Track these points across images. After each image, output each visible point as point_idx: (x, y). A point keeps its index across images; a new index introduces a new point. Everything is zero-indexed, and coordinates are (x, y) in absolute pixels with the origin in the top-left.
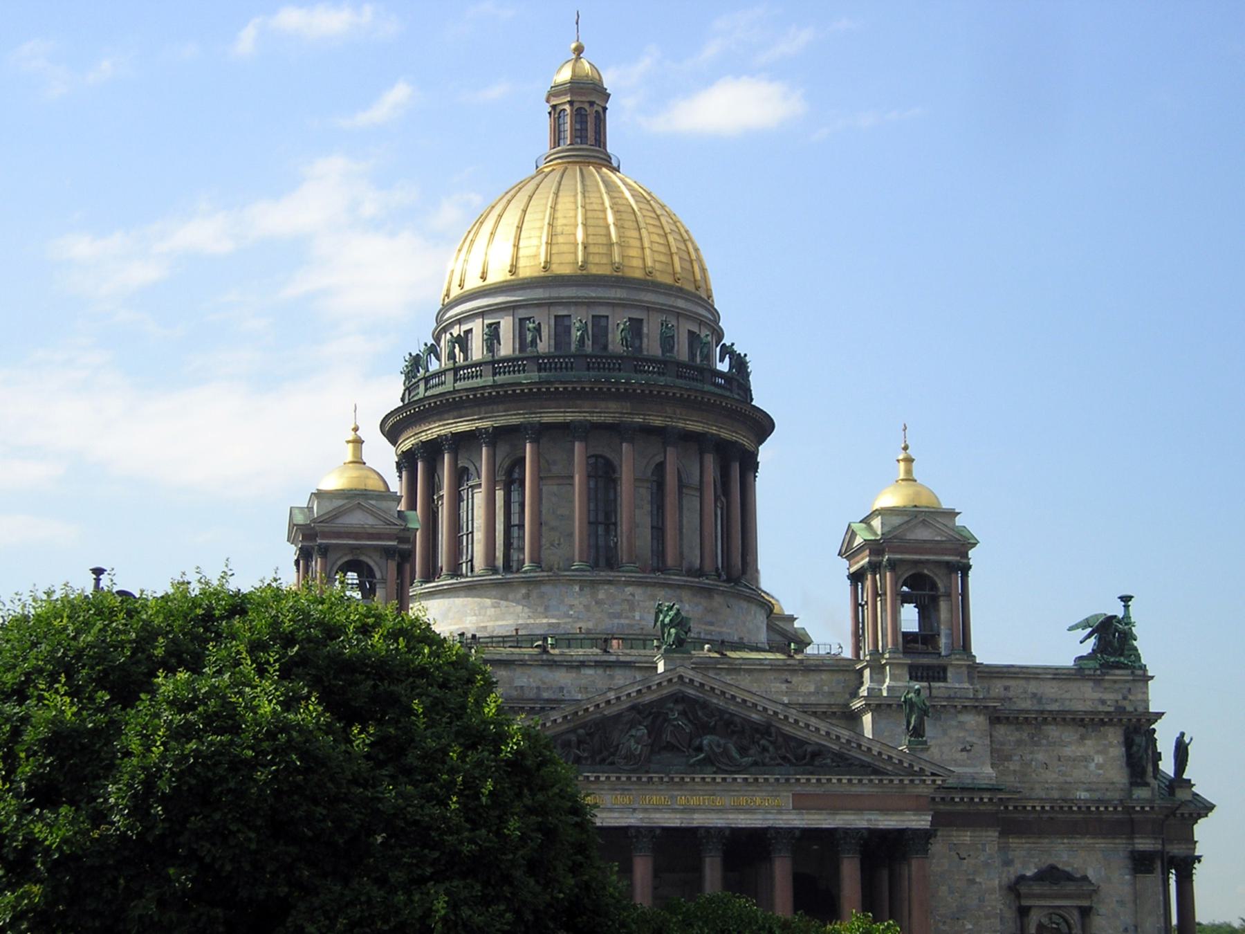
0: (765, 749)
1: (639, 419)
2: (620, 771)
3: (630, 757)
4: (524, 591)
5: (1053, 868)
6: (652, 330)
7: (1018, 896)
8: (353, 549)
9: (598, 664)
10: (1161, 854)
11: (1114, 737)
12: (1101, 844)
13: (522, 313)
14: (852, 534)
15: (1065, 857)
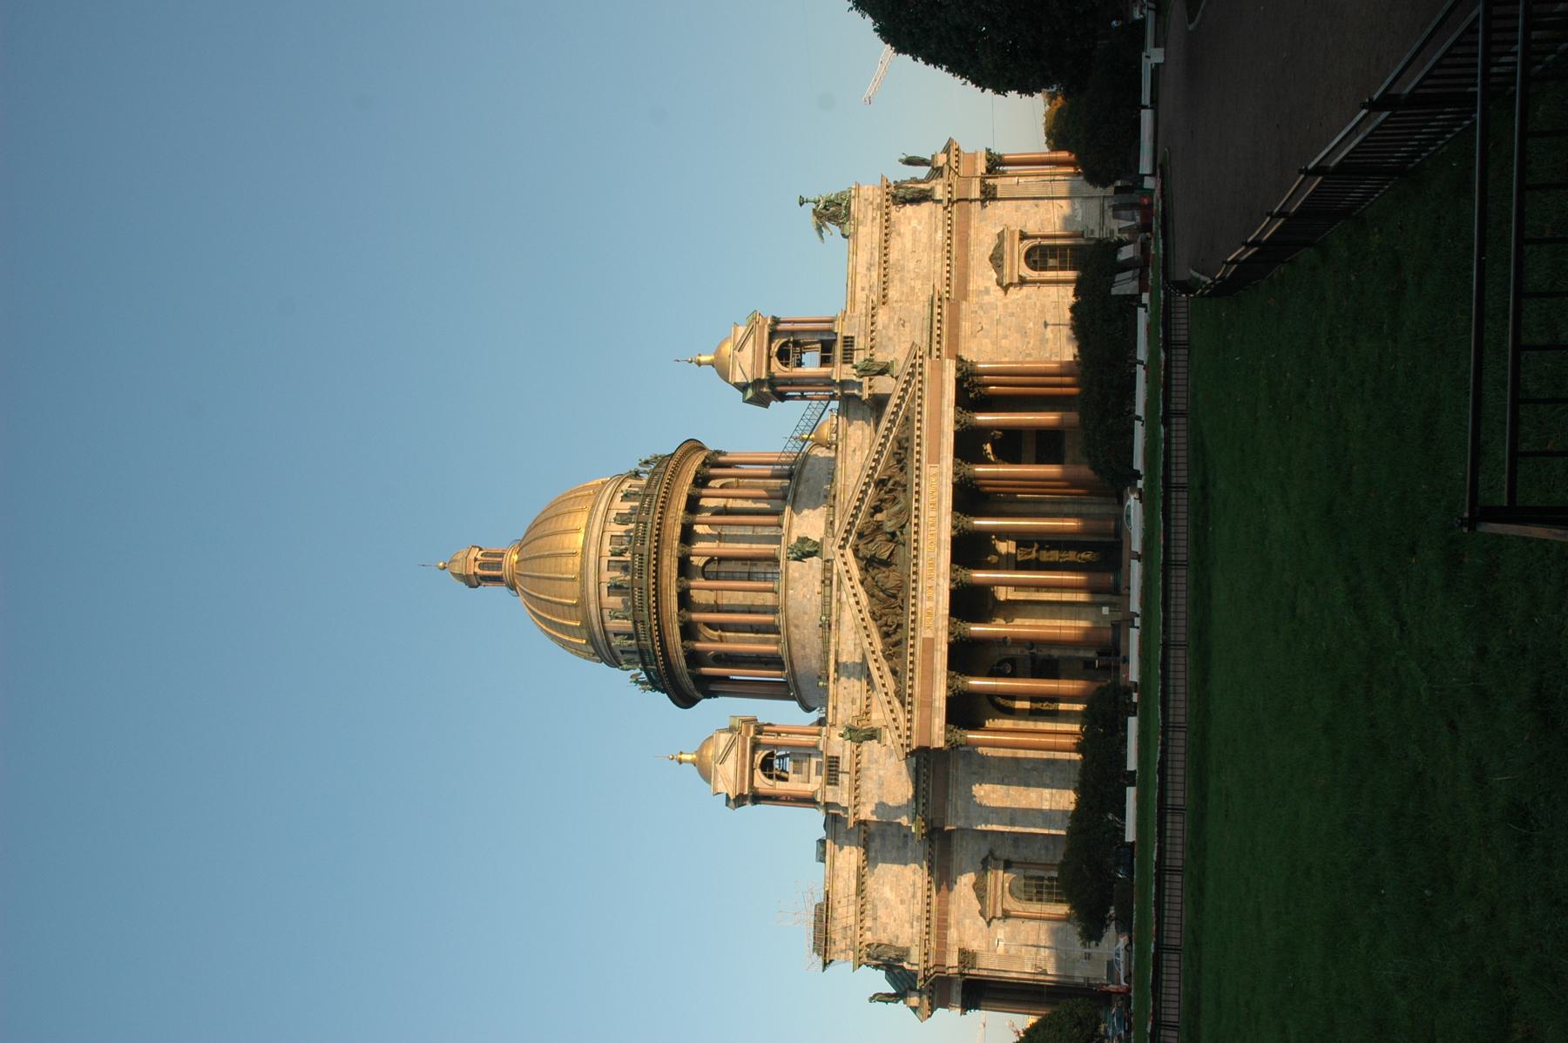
0: (895, 483)
1: (676, 543)
2: (907, 596)
3: (899, 588)
4: (792, 629)
5: (991, 259)
6: (619, 530)
7: (1011, 284)
8: (752, 770)
9: (839, 589)
10: (982, 182)
11: (897, 213)
12: (974, 223)
13: (607, 618)
14: (750, 401)
15: (983, 249)
